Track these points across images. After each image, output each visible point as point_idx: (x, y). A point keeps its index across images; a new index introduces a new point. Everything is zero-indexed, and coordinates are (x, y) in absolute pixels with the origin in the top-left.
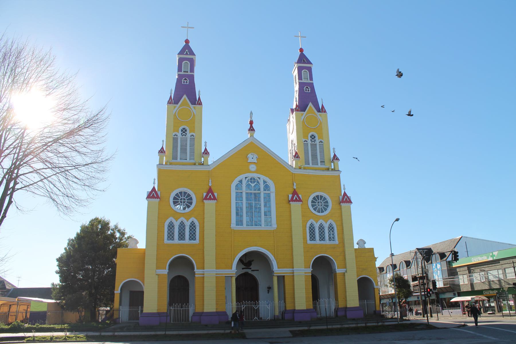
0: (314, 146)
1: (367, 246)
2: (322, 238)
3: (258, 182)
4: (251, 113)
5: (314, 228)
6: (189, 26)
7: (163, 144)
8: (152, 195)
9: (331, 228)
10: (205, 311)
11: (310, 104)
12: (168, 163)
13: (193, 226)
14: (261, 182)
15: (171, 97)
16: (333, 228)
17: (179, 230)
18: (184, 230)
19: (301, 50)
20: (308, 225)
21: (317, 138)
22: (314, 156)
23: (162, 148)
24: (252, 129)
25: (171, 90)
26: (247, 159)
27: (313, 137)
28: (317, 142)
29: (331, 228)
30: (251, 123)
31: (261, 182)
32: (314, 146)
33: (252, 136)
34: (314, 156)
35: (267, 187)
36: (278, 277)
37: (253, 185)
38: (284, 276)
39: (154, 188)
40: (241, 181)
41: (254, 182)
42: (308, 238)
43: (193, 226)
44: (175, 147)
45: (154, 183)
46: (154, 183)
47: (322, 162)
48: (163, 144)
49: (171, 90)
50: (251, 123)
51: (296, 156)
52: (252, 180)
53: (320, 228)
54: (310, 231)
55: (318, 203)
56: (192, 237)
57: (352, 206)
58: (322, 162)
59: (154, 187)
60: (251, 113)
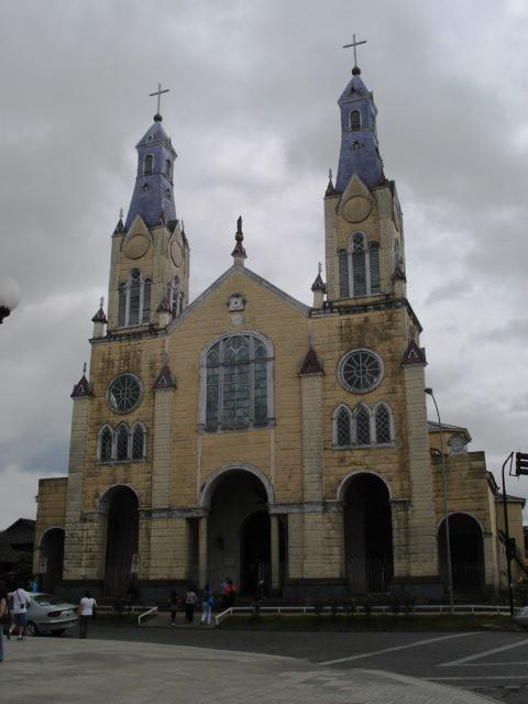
0: (359, 255)
1: (471, 447)
2: (363, 437)
3: (246, 346)
4: (240, 221)
5: (347, 419)
6: (162, 89)
7: (101, 305)
8: (82, 391)
9: (382, 416)
10: (151, 578)
11: (355, 177)
12: (111, 336)
13: (139, 435)
14: (251, 341)
15: (120, 223)
16: (387, 416)
17: (119, 443)
18: (126, 443)
19: (356, 72)
20: (335, 416)
21: (365, 242)
22: (360, 279)
23: (101, 312)
24: (239, 252)
25: (122, 211)
26: (228, 305)
27: (358, 239)
28: (366, 247)
29: (382, 416)
30: (239, 238)
31: (251, 343)
32: (359, 255)
33: (238, 265)
34: (360, 279)
35: (261, 351)
36: (278, 516)
37: (236, 351)
38: (285, 515)
39: (84, 378)
40: (216, 346)
41: (240, 345)
42: (335, 441)
43: (139, 435)
44: (122, 304)
45: (85, 370)
46: (85, 370)
47: (375, 286)
48: (101, 305)
49: (122, 211)
50: (239, 238)
51: (318, 287)
52: (237, 340)
53: (358, 419)
54: (339, 426)
55: (359, 368)
56: (137, 455)
57: (426, 369)
58: (375, 286)
59: (84, 378)
60: (240, 221)
